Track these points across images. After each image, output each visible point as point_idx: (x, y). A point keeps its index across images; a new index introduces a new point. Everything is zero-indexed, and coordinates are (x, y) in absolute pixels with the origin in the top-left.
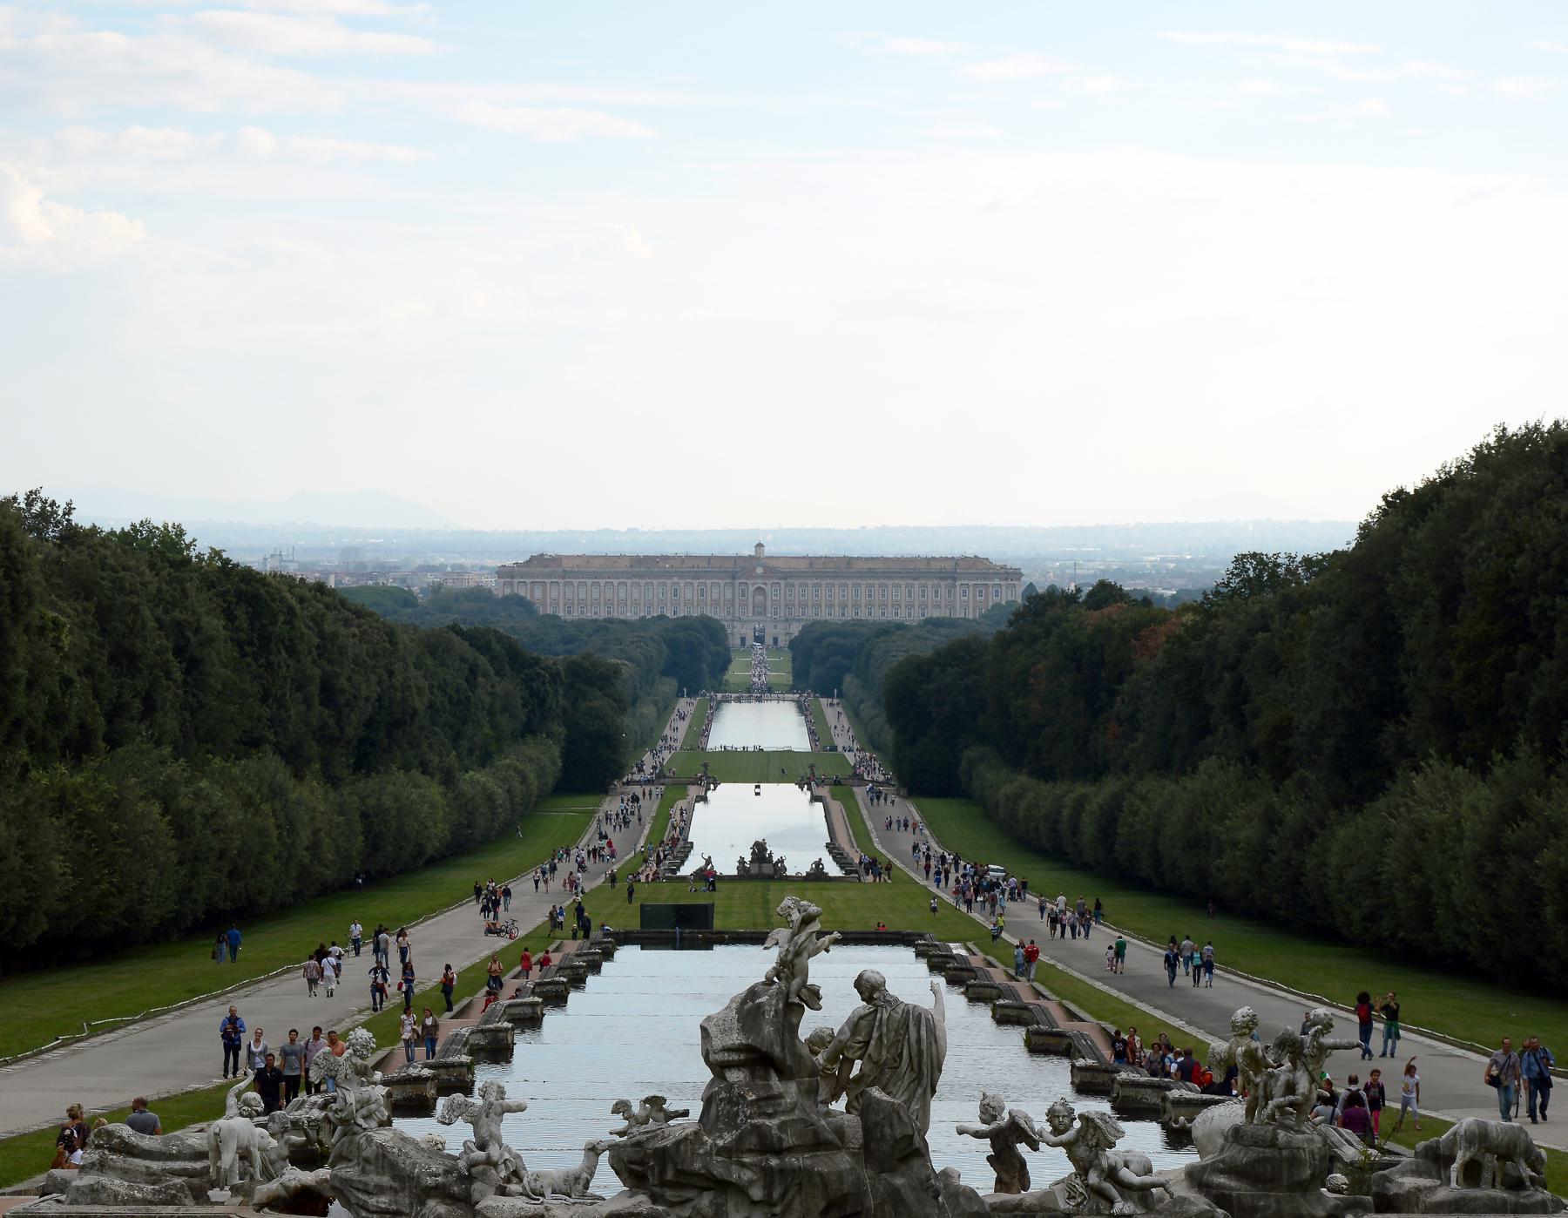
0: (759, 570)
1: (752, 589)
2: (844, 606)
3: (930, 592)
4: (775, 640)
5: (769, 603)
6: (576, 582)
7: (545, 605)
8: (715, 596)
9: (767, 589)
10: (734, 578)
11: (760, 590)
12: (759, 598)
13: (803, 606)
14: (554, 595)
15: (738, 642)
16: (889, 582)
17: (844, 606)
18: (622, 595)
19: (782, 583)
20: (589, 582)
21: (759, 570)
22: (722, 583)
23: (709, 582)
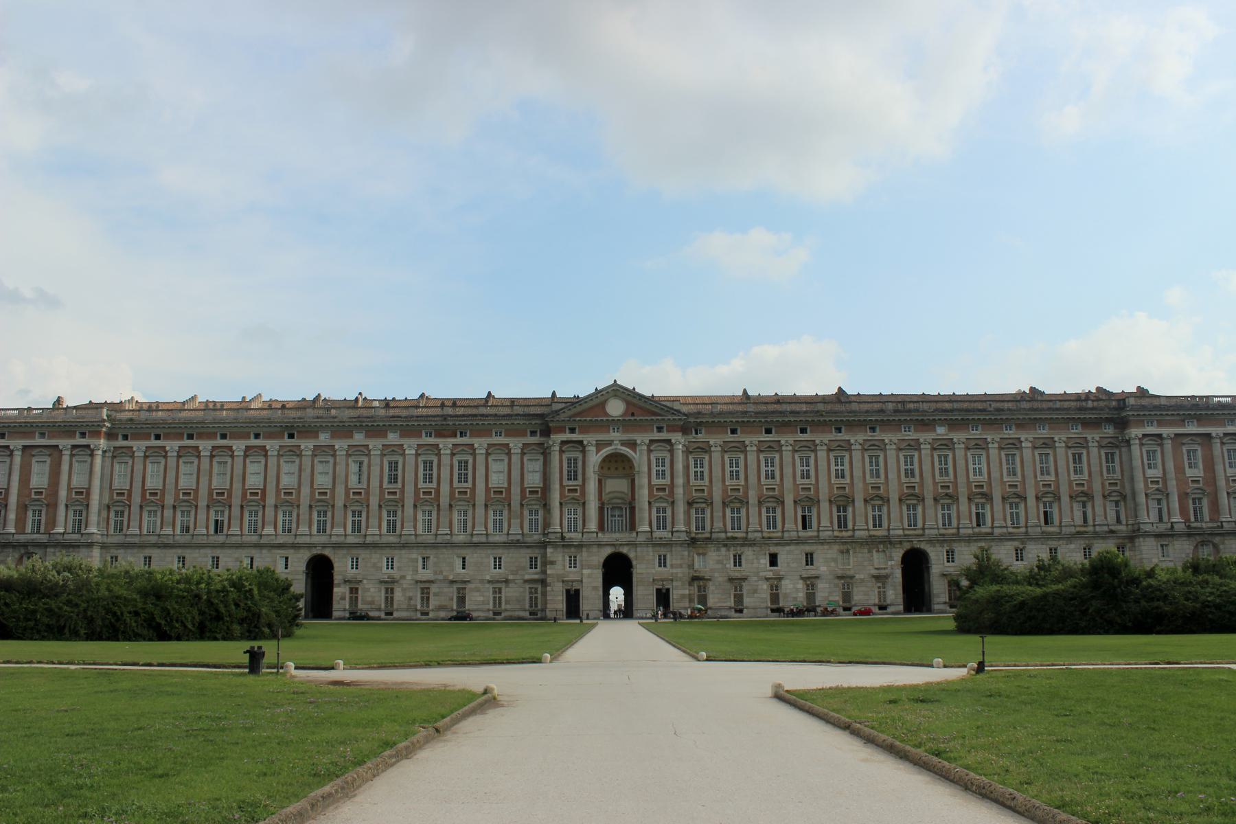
0: (616, 408)
1: (595, 458)
2: (843, 502)
3: (1062, 455)
4: (663, 597)
5: (643, 494)
7: (52, 506)
8: (497, 480)
9: (639, 458)
10: (546, 432)
11: (617, 464)
12: (616, 486)
13: (736, 501)
15: (557, 601)
16: (958, 436)
18: (254, 481)
21: (616, 408)
22: (515, 444)
23: (480, 443)
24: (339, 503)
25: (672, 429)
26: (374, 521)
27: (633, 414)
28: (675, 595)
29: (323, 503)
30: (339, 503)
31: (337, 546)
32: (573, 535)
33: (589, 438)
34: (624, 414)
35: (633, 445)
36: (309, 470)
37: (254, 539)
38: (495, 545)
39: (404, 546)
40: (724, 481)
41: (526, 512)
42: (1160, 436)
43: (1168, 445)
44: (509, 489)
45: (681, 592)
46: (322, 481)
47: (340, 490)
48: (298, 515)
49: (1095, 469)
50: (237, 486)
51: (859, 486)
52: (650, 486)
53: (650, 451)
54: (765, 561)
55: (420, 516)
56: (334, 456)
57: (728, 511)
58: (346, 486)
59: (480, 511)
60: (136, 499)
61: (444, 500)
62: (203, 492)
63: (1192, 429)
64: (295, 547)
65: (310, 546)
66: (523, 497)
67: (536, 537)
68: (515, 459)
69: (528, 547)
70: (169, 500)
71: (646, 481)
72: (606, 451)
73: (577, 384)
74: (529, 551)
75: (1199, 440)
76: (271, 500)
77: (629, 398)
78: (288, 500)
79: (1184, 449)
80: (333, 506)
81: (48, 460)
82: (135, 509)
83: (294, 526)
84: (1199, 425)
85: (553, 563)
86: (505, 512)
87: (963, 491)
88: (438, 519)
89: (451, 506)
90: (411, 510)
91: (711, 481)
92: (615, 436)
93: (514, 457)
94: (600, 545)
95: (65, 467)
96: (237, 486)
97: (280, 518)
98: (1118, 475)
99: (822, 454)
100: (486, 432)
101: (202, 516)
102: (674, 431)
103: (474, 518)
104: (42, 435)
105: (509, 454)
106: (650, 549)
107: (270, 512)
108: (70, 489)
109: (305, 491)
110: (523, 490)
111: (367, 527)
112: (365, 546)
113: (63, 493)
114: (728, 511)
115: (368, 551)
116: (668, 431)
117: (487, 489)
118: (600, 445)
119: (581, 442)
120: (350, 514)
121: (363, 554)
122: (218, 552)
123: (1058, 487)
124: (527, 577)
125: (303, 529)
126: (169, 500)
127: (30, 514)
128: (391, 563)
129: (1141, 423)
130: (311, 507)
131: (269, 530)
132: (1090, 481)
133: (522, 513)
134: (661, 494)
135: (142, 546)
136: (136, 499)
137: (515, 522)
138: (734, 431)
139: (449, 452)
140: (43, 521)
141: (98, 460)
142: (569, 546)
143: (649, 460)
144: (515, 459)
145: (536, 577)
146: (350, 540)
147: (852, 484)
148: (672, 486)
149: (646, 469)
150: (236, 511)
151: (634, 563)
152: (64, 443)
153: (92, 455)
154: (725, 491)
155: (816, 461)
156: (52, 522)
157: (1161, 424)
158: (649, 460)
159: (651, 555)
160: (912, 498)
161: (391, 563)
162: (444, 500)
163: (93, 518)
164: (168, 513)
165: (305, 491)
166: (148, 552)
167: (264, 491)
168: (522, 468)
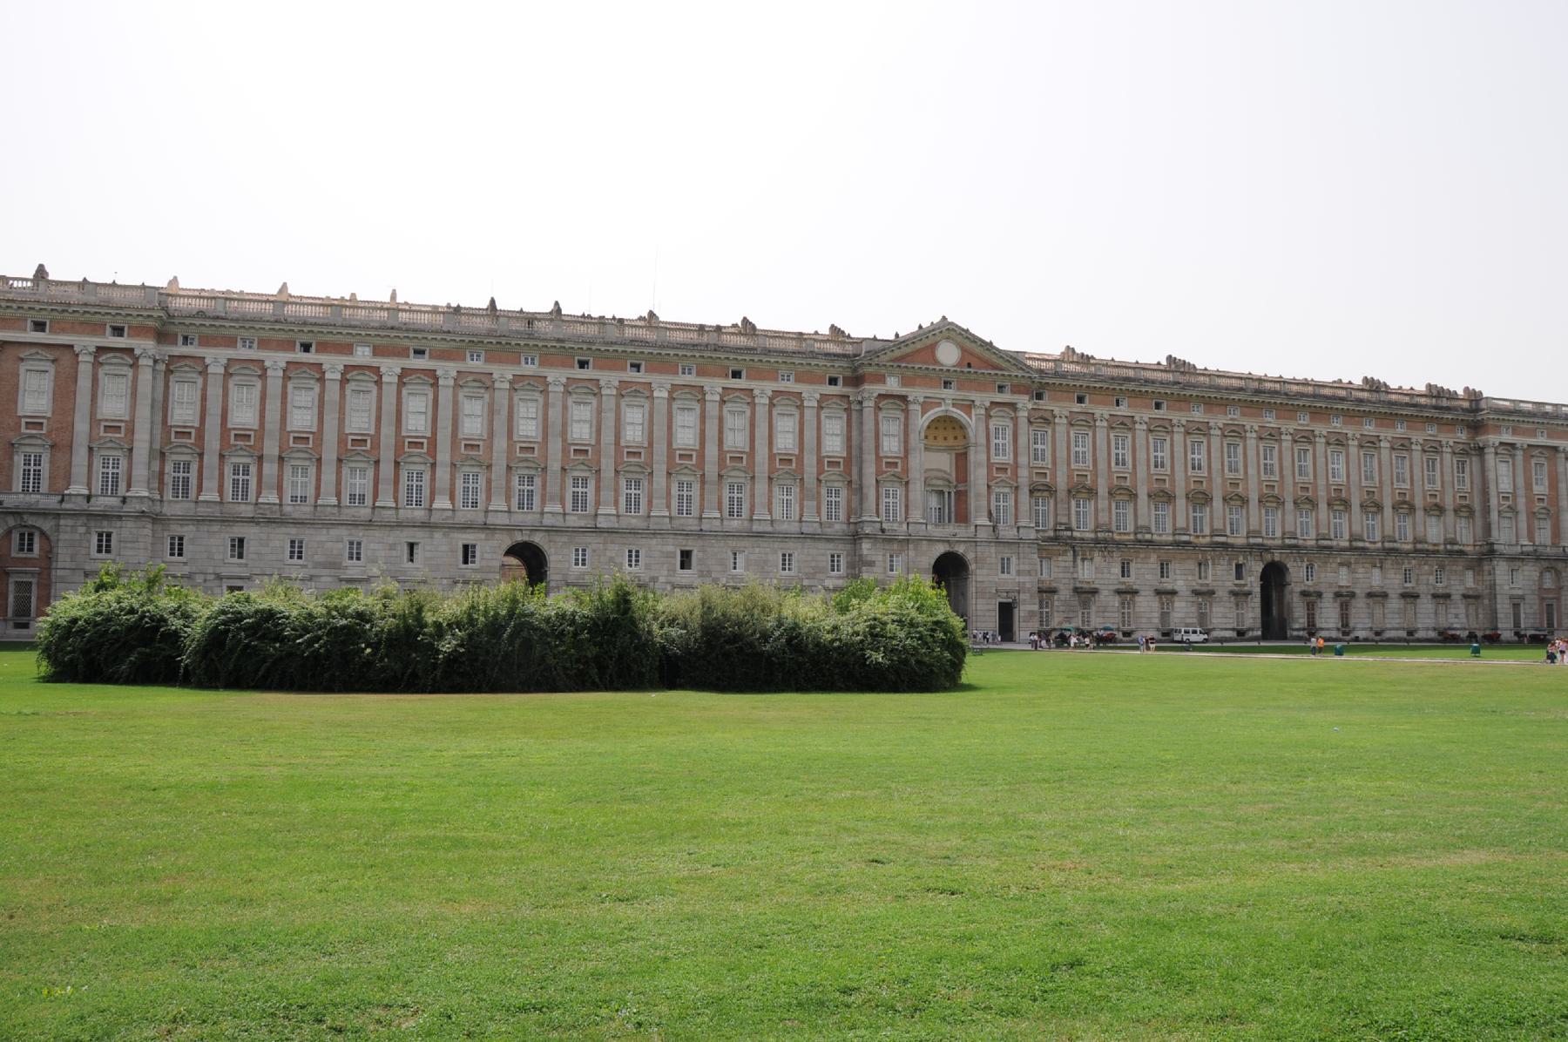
0: (948, 355)
1: (921, 421)
6: (216, 357)
7: (61, 447)
8: (786, 442)
9: (973, 422)
10: (856, 380)
13: (1082, 490)
14: (113, 406)
17: (1200, 498)
19: (1024, 402)
20: (276, 360)
21: (948, 355)
24: (555, 465)
25: (1017, 390)
26: (607, 495)
27: (969, 365)
28: (1020, 613)
29: (527, 461)
30: (555, 465)
31: (551, 530)
32: (895, 526)
33: (916, 393)
34: (959, 365)
35: (968, 407)
36: (505, 412)
37: (419, 514)
38: (786, 537)
39: (654, 534)
40: (1069, 464)
41: (824, 491)
42: (1513, 445)
43: (1519, 454)
44: (800, 458)
45: (1029, 608)
46: (528, 428)
47: (555, 446)
48: (489, 482)
49: (1448, 478)
50: (388, 431)
51: (1218, 480)
52: (990, 465)
53: (988, 417)
54: (1117, 570)
55: (675, 491)
56: (545, 392)
57: (1073, 503)
58: (564, 440)
59: (761, 487)
60: (213, 443)
61: (711, 469)
62: (331, 437)
63: (1541, 440)
64: (485, 527)
65: (509, 529)
66: (820, 471)
67: (837, 527)
68: (810, 415)
69: (828, 540)
70: (271, 448)
71: (984, 457)
72: (933, 413)
73: (880, 318)
74: (831, 546)
75: (1547, 453)
76: (444, 456)
77: (968, 344)
78: (471, 453)
79: (1533, 461)
80: (545, 469)
81: (51, 368)
82: (211, 459)
83: (481, 498)
84: (1549, 437)
85: (871, 564)
86: (796, 490)
87: (1322, 494)
88: (702, 495)
89: (720, 476)
90: (663, 481)
91: (1054, 463)
92: (950, 394)
93: (807, 412)
94: (931, 541)
95: (84, 383)
96: (388, 431)
97: (459, 484)
98: (1468, 487)
99: (1178, 438)
100: (772, 375)
101: (329, 475)
102: (1019, 392)
103: (753, 496)
104: (40, 326)
105: (801, 407)
106: (993, 550)
107: (443, 474)
108: (94, 421)
109: (500, 444)
110: (820, 460)
111: (598, 503)
112: (596, 530)
113: (81, 426)
114: (1073, 503)
115: (601, 540)
116: (1013, 392)
117: (772, 457)
118: (926, 407)
119: (904, 398)
120: (569, 482)
121: (593, 542)
122: (358, 535)
123: (1413, 496)
124: (830, 583)
125: (498, 504)
126: (271, 448)
127: (19, 460)
128: (634, 557)
129: (1497, 429)
130: (509, 468)
131: (442, 503)
132: (1443, 492)
133: (819, 493)
134: (1003, 476)
135: (228, 521)
136: (213, 443)
137: (810, 505)
138: (1081, 400)
139: (717, 398)
140: (45, 474)
141: (146, 376)
142: (890, 541)
143: (987, 428)
144: (810, 415)
145: (840, 583)
146: (572, 521)
147: (1210, 479)
148: (1016, 465)
149: (984, 441)
150: (387, 469)
151: (972, 567)
152: (85, 343)
153: (134, 366)
154: (1070, 477)
155: (1172, 445)
156: (63, 475)
157: (1515, 432)
158: (987, 428)
159: (992, 554)
160: (1271, 500)
161: (634, 557)
162: (711, 469)
163: (140, 472)
164: (270, 469)
165: (500, 444)
166: (238, 531)
167: (433, 441)
168: (819, 429)
